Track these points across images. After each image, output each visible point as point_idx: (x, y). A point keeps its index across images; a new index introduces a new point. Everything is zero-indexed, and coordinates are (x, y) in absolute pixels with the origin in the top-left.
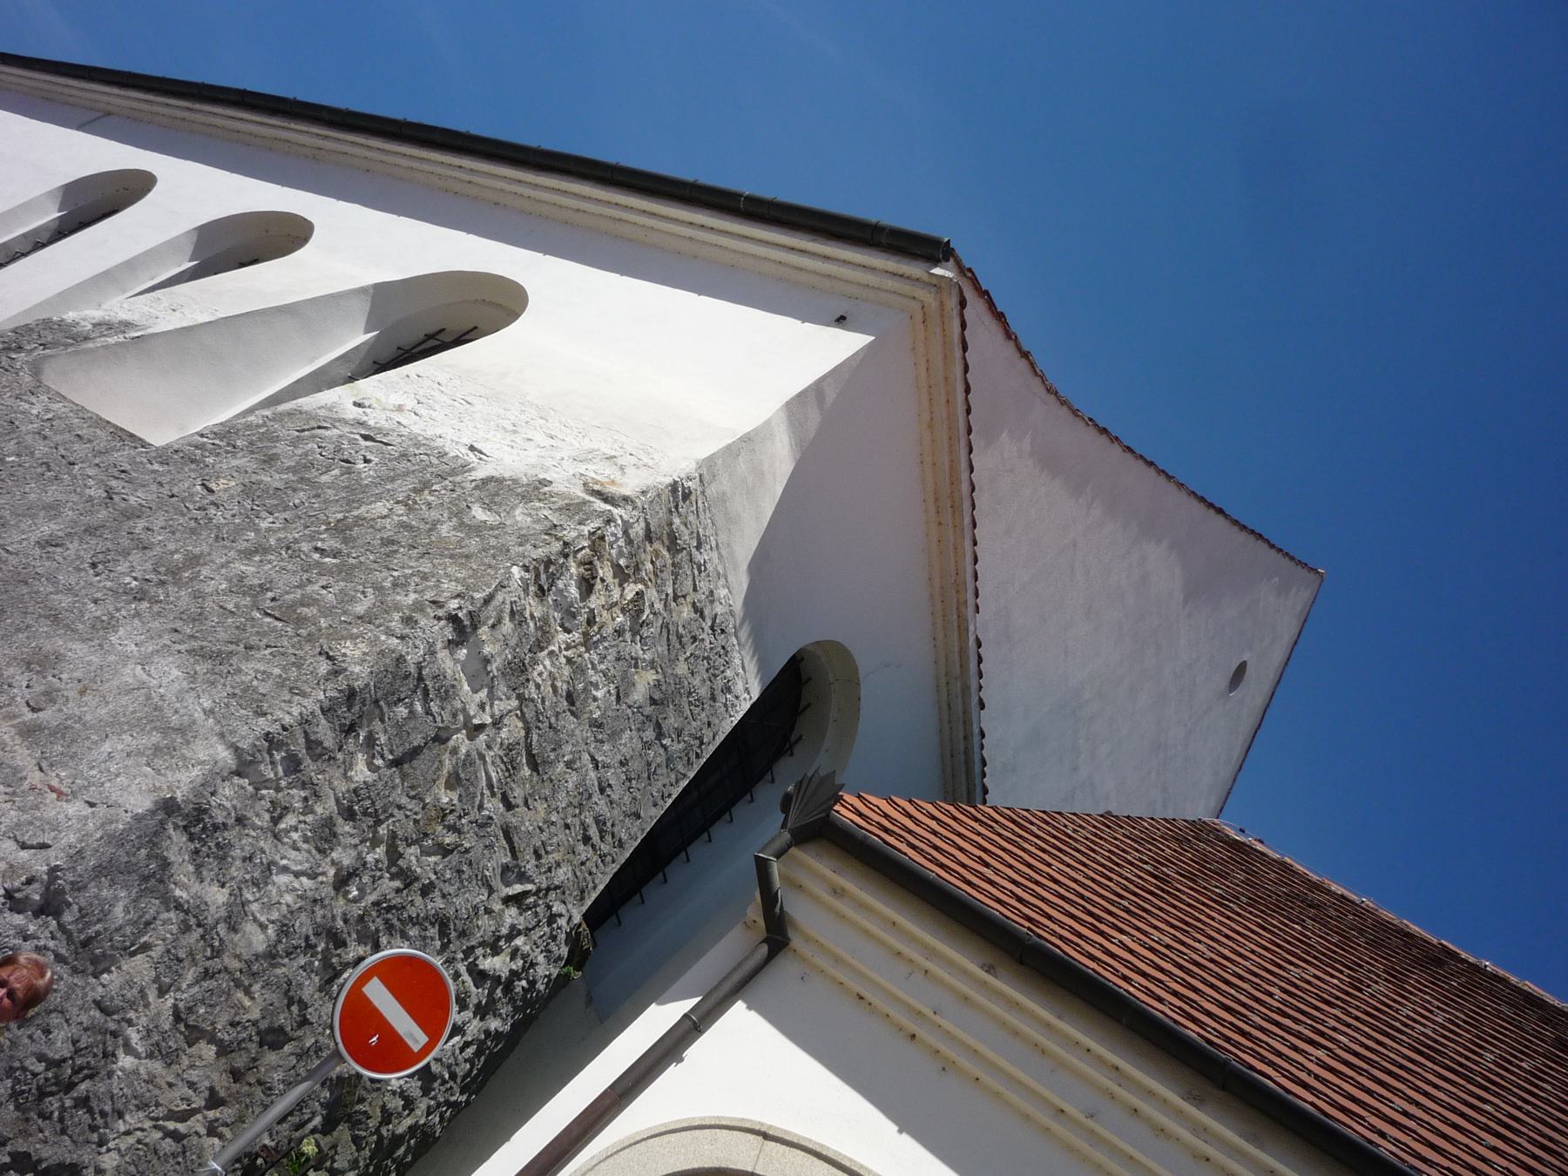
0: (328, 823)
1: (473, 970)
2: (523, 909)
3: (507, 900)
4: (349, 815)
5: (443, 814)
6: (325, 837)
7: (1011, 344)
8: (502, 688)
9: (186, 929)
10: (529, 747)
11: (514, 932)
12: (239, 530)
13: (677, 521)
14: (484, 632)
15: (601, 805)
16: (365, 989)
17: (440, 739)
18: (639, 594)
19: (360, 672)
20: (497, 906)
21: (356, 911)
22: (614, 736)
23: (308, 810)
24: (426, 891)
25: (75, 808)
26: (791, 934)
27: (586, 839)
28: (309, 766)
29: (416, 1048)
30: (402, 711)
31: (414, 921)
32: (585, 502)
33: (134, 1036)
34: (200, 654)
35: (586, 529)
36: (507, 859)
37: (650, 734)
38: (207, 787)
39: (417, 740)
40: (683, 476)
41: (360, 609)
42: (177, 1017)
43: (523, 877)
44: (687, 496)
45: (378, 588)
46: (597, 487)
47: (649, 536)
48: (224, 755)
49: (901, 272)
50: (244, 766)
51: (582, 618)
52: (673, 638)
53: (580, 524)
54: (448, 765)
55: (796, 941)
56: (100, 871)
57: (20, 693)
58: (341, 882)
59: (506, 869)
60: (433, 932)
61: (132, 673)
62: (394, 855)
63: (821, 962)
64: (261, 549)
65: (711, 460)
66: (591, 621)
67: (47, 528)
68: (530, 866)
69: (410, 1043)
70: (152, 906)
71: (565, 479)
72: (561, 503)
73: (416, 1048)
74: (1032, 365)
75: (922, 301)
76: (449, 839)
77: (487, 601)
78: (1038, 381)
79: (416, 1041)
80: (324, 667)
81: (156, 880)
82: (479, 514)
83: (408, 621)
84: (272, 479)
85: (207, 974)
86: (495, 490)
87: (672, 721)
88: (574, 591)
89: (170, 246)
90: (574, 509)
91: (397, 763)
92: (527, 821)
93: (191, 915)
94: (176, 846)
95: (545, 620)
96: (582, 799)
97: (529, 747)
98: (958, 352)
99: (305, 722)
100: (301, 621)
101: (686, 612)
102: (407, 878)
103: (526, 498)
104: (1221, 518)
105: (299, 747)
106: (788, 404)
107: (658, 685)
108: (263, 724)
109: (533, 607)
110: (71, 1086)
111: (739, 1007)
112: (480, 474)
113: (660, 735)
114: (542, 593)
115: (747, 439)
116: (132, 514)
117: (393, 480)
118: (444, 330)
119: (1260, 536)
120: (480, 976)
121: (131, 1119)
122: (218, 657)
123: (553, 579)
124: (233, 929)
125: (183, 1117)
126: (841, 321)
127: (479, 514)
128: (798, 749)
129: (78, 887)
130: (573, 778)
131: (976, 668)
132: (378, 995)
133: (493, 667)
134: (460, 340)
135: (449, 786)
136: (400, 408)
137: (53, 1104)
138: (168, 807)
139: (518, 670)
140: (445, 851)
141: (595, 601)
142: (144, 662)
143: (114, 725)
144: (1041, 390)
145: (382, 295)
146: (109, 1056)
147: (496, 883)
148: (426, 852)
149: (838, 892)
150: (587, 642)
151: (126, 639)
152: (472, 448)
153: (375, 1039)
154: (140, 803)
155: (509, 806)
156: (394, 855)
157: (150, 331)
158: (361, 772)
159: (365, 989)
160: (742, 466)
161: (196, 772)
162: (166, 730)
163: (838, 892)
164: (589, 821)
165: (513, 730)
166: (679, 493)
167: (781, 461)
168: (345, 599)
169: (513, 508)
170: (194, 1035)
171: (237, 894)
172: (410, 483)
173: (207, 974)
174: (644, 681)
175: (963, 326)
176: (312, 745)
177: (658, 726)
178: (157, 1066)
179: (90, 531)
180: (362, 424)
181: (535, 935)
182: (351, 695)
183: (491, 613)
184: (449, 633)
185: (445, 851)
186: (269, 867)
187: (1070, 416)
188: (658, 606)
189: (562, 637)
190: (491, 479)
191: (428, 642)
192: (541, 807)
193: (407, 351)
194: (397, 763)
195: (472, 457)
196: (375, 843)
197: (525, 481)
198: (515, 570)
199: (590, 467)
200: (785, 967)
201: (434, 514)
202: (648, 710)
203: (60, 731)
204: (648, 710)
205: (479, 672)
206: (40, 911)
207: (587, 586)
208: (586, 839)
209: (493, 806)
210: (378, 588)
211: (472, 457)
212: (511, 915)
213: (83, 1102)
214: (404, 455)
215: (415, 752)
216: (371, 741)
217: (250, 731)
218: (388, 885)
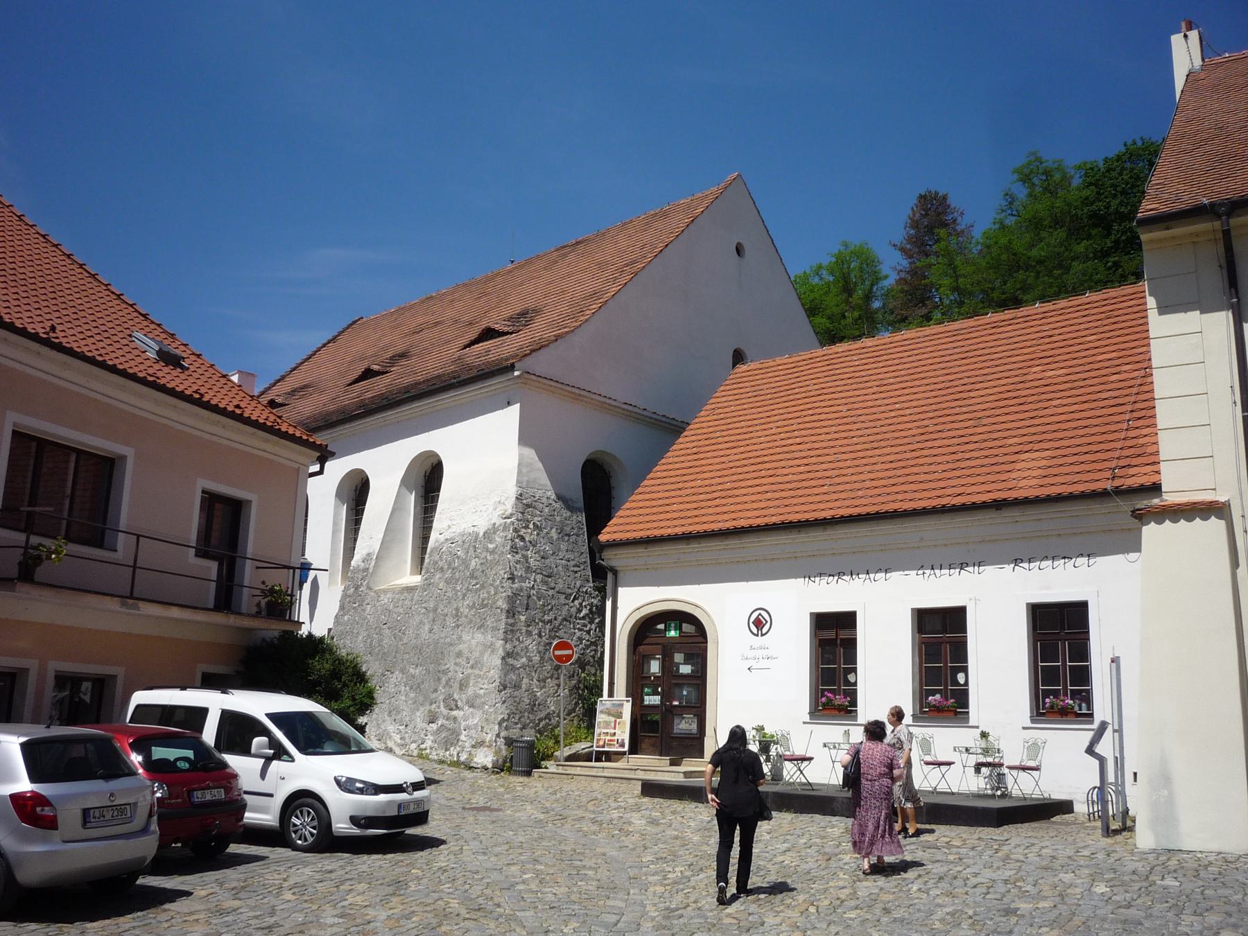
0: (527, 631)
1: (580, 619)
2: (578, 599)
3: (573, 601)
4: (529, 626)
5: (544, 605)
6: (529, 633)
8: (529, 575)
9: (525, 669)
10: (545, 576)
11: (581, 604)
12: (456, 594)
13: (525, 501)
14: (515, 573)
15: (572, 563)
17: (529, 597)
18: (534, 524)
19: (505, 606)
20: (572, 604)
21: (547, 636)
22: (559, 550)
23: (521, 634)
24: (555, 619)
25: (492, 672)
27: (576, 572)
28: (515, 628)
30: (518, 602)
31: (560, 625)
32: (505, 523)
33: (535, 689)
34: (479, 628)
35: (511, 531)
36: (564, 596)
37: (566, 538)
38: (505, 649)
39: (526, 602)
41: (493, 593)
42: (539, 681)
43: (571, 595)
44: (521, 495)
45: (492, 585)
47: (523, 513)
48: (501, 642)
50: (506, 641)
51: (528, 544)
52: (550, 518)
54: (535, 598)
56: (505, 676)
57: (464, 663)
58: (540, 635)
59: (566, 598)
60: (565, 623)
61: (474, 642)
62: (543, 622)
64: (464, 595)
65: (518, 482)
66: (531, 542)
67: (427, 627)
68: (570, 591)
70: (517, 672)
72: (501, 528)
76: (549, 607)
77: (510, 568)
80: (499, 611)
81: (513, 668)
82: (491, 546)
83: (502, 587)
84: (448, 574)
85: (536, 671)
87: (568, 529)
88: (522, 543)
89: (336, 507)
90: (505, 528)
91: (527, 609)
92: (560, 586)
93: (524, 667)
94: (510, 661)
95: (523, 555)
96: (566, 568)
97: (545, 576)
98: (540, 379)
99: (506, 624)
100: (486, 605)
101: (546, 510)
102: (550, 621)
103: (495, 533)
105: (510, 628)
106: (519, 444)
107: (557, 529)
108: (501, 631)
109: (518, 557)
110: (535, 705)
111: (620, 589)
112: (481, 534)
113: (569, 535)
114: (517, 553)
115: (519, 465)
116: (435, 610)
117: (468, 552)
120: (583, 618)
121: (549, 700)
122: (482, 626)
123: (516, 548)
124: (532, 661)
125: (557, 692)
126: (509, 404)
127: (491, 546)
129: (505, 681)
130: (560, 568)
132: (558, 653)
133: (524, 575)
135: (540, 601)
137: (535, 709)
138: (503, 658)
139: (528, 569)
140: (551, 609)
141: (527, 539)
142: (473, 638)
143: (482, 654)
145: (404, 482)
146: (535, 696)
147: (567, 602)
148: (548, 614)
149: (616, 555)
150: (534, 546)
151: (466, 637)
154: (500, 661)
155: (554, 589)
156: (543, 622)
157: (376, 552)
158: (523, 618)
160: (524, 470)
161: (501, 649)
162: (489, 647)
163: (616, 555)
164: (573, 569)
165: (539, 578)
166: (519, 498)
167: (531, 453)
168: (488, 593)
170: (544, 681)
171: (526, 656)
172: (472, 550)
173: (536, 671)
174: (554, 534)
176: (511, 625)
177: (566, 535)
178: (544, 690)
179: (434, 621)
180: (447, 540)
181: (586, 599)
182: (508, 611)
183: (513, 568)
184: (511, 581)
185: (551, 609)
186: (526, 648)
188: (540, 519)
189: (529, 552)
190: (484, 533)
192: (560, 580)
194: (527, 609)
196: (538, 624)
198: (509, 556)
200: (620, 575)
201: (483, 556)
202: (560, 536)
203: (476, 663)
204: (560, 536)
205: (523, 579)
206: (505, 689)
207: (522, 539)
208: (576, 572)
209: (551, 592)
210: (492, 585)
211: (476, 529)
212: (576, 602)
213: (539, 705)
215: (528, 604)
216: (519, 612)
217: (501, 634)
218: (548, 626)
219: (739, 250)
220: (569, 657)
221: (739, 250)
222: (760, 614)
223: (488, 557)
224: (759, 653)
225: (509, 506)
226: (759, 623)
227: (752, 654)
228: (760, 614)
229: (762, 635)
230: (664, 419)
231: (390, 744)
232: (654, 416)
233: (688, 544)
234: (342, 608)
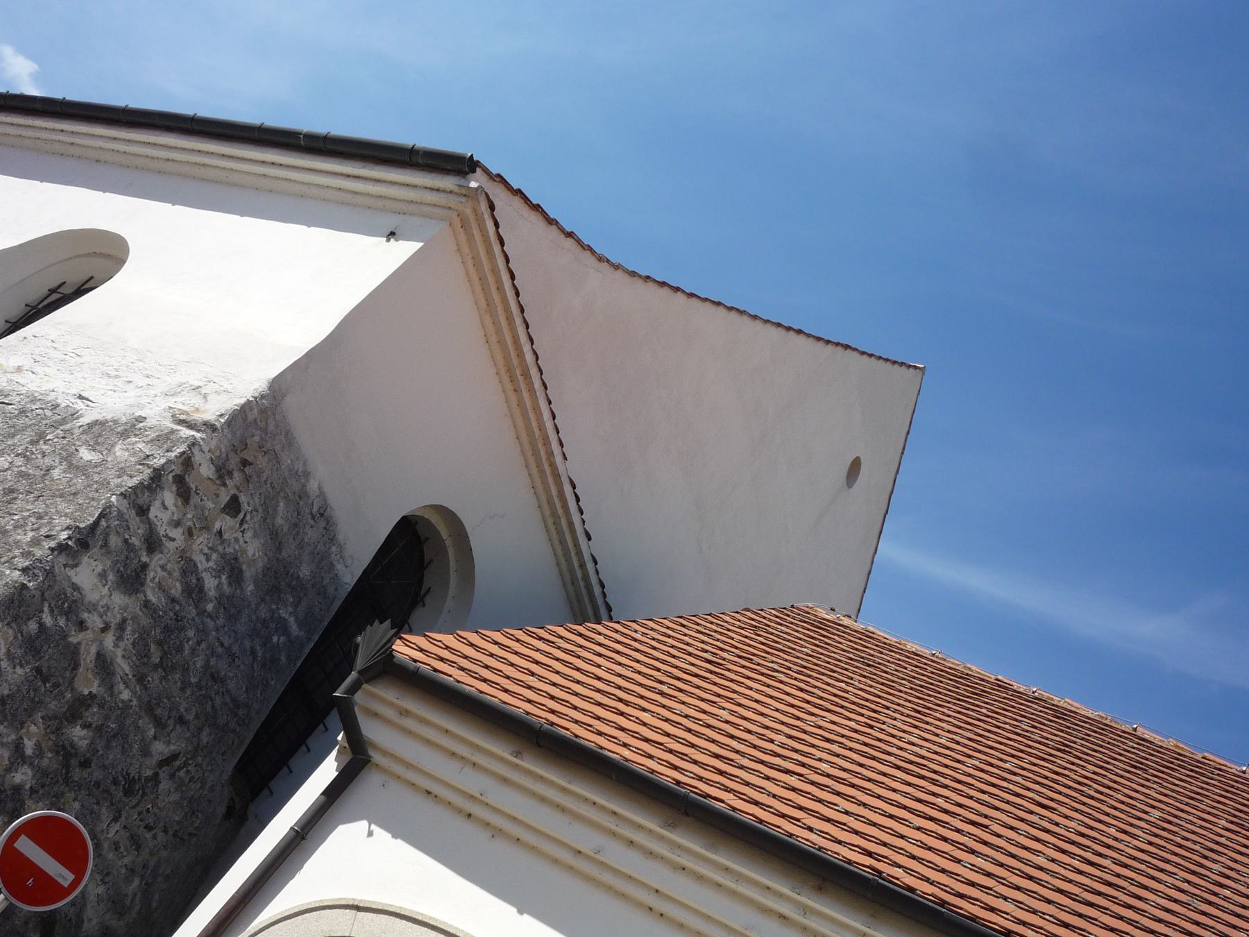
7: (554, 227)
16: (16, 845)
24: (85, 764)
26: (371, 753)
29: (66, 884)
32: (173, 432)
40: (256, 395)
46: (182, 417)
49: (436, 187)
53: (168, 451)
55: (376, 757)
63: (398, 769)
69: (60, 881)
71: (156, 414)
72: (153, 435)
73: (66, 884)
74: (579, 241)
75: (457, 210)
78: (588, 253)
79: (65, 879)
82: (86, 455)
86: (100, 432)
90: (165, 438)
103: (124, 435)
104: (802, 336)
112: (86, 420)
117: (13, 436)
118: (64, 283)
119: (847, 347)
127: (86, 455)
128: (428, 600)
131: (576, 506)
134: (80, 291)
136: (19, 369)
144: (593, 260)
149: (405, 713)
152: (81, 397)
153: (30, 881)
159: (16, 845)
163: (405, 713)
169: (113, 446)
172: (29, 435)
175: (497, 225)
187: (627, 278)
191: (46, 570)
193: (34, 308)
195: (80, 405)
197: (124, 420)
199: (179, 399)
201: (48, 461)
211: (80, 405)
214: (23, 412)
219: (855, 467)
221: (855, 467)
223: (56, 473)
225: (215, 408)
230: (597, 590)
232: (590, 566)
233: (671, 825)
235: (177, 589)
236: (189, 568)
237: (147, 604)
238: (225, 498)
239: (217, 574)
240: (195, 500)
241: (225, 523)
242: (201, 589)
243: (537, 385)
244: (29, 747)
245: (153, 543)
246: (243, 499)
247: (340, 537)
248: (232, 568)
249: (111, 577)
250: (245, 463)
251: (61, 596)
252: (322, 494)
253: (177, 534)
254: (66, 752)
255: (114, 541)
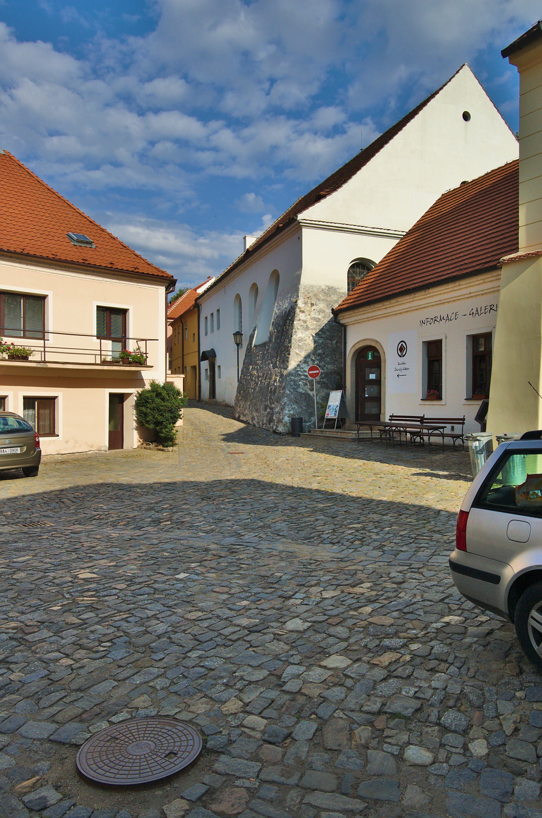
132: (310, 372)
219: (466, 116)
220: (317, 374)
221: (466, 116)
222: (402, 344)
224: (403, 366)
226: (401, 349)
227: (398, 367)
228: (402, 344)
229: (403, 356)
231: (255, 422)
234: (246, 356)
235: (315, 323)
236: (315, 319)
237: (312, 329)
238: (310, 305)
239: (319, 315)
240: (305, 311)
241: (314, 307)
242: (319, 319)
243: (346, 226)
244: (313, 358)
245: (305, 322)
246: (313, 302)
247: (337, 287)
248: (321, 311)
249: (303, 332)
250: (308, 298)
251: (299, 340)
252: (327, 286)
253: (308, 317)
254: (319, 355)
255: (299, 327)
